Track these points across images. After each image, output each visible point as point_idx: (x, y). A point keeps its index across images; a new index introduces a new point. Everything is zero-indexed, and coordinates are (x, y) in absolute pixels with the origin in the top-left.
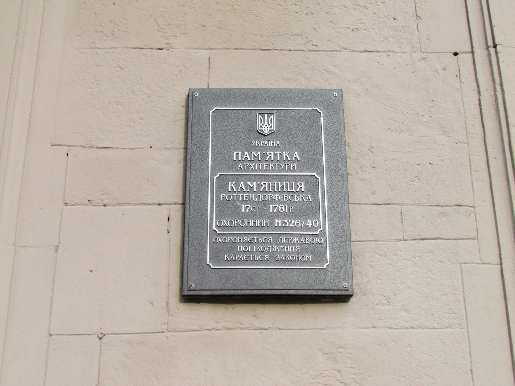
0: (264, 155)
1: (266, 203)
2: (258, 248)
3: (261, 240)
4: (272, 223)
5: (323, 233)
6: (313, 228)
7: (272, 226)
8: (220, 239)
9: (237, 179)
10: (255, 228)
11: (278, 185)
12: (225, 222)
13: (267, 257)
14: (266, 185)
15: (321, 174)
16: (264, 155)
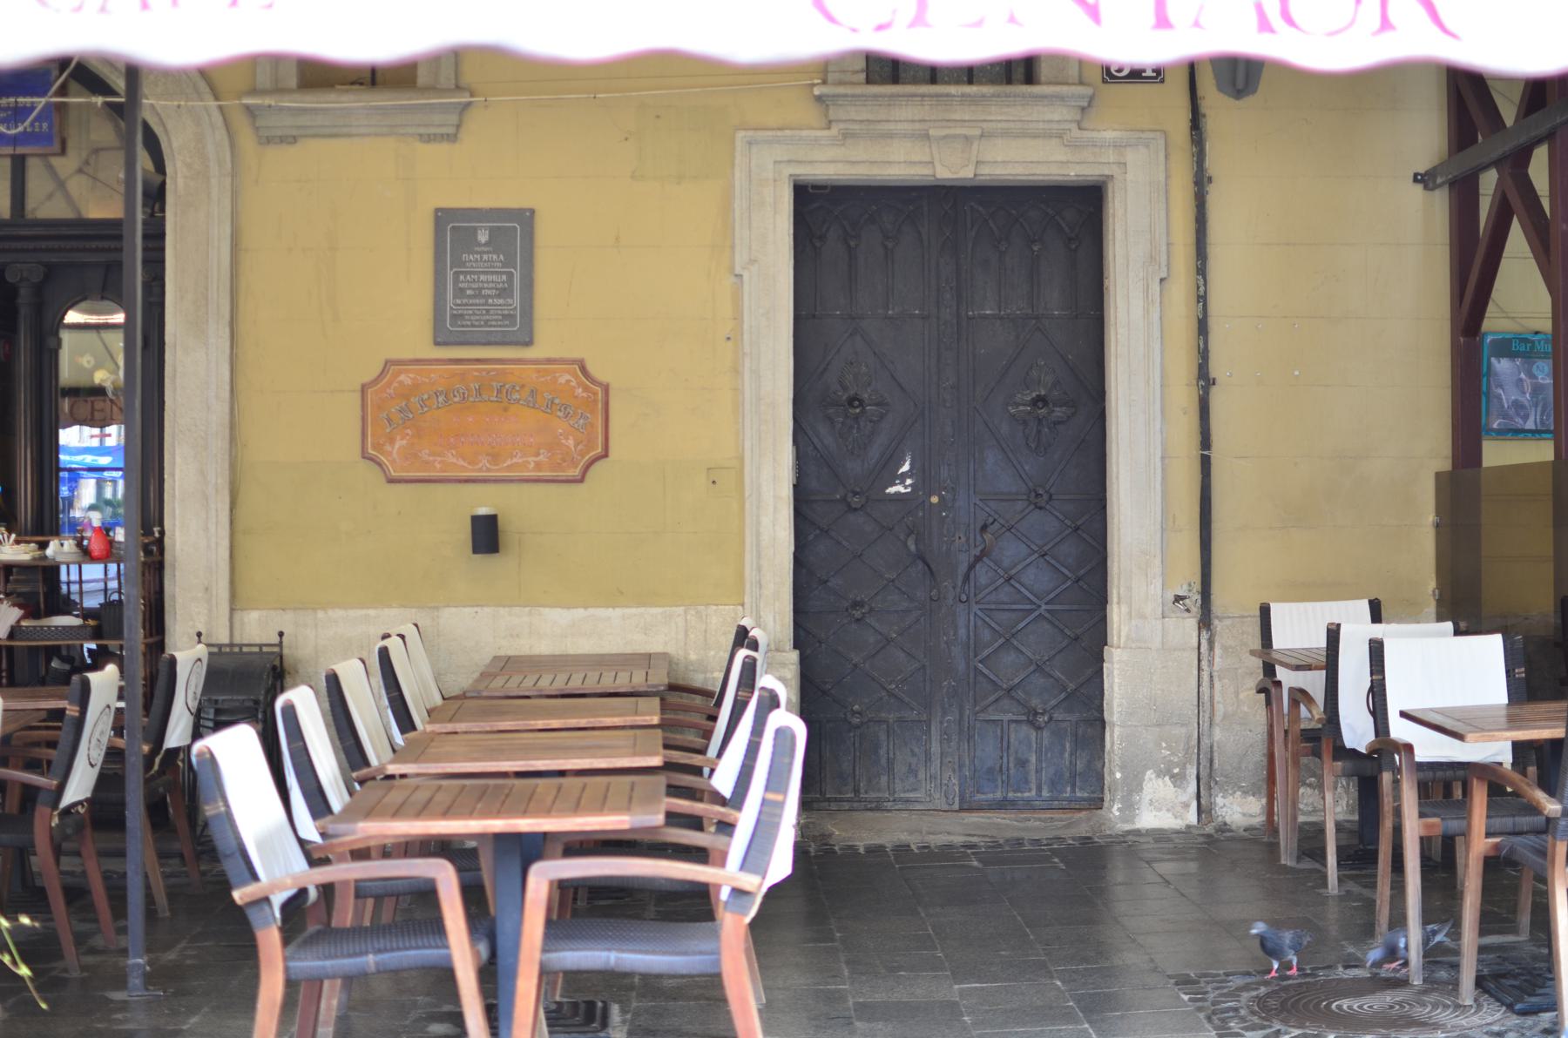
0: (481, 258)
1: (480, 289)
2: (478, 318)
3: (478, 313)
4: (487, 301)
5: (516, 308)
6: (511, 305)
7: (486, 304)
8: (455, 312)
9: (465, 273)
10: (476, 305)
11: (490, 278)
12: (458, 301)
13: (482, 323)
14: (482, 277)
15: (516, 270)
16: (481, 258)
